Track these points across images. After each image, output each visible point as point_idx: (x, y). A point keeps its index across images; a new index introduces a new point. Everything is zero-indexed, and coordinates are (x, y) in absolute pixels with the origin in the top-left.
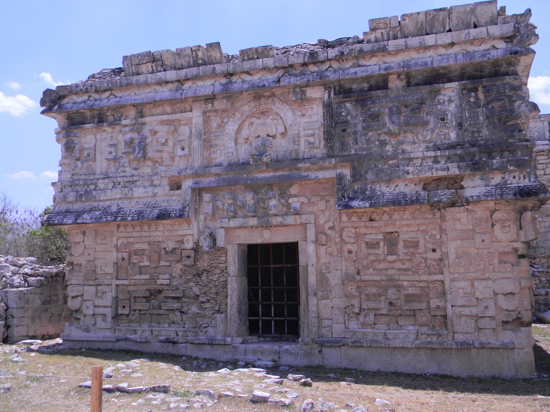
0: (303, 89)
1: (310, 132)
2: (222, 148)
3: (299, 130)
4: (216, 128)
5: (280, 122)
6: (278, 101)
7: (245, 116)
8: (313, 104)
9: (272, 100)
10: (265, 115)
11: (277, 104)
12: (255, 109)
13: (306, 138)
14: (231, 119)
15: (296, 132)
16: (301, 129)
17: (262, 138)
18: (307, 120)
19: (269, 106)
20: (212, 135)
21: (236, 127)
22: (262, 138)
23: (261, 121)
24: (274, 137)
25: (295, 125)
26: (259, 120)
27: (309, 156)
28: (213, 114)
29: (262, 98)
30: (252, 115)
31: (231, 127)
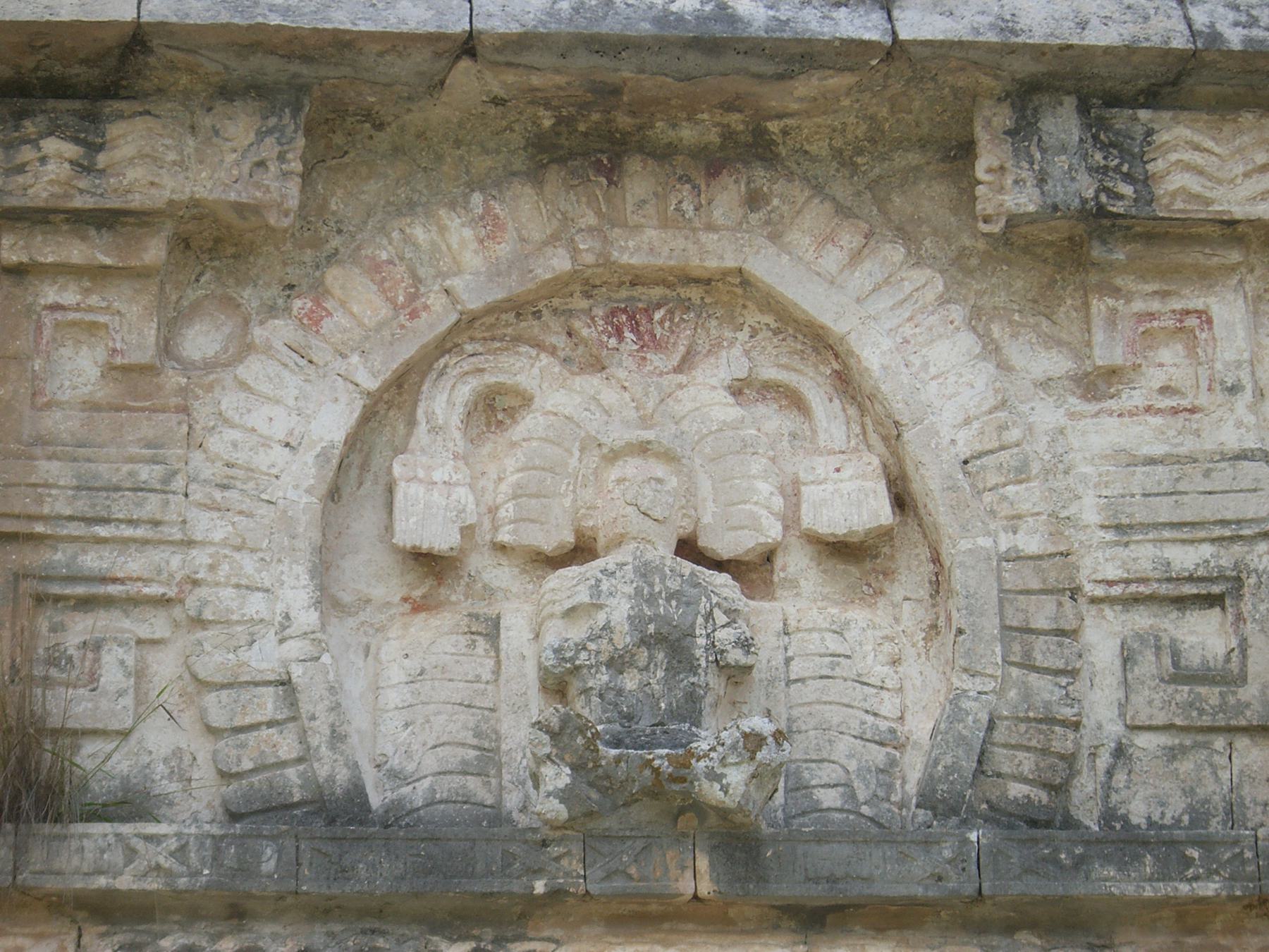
0: (1120, 118)
1: (1186, 558)
2: (155, 625)
3: (1059, 523)
4: (92, 406)
5: (830, 418)
6: (816, 214)
7: (438, 316)
8: (1206, 277)
9: (754, 200)
10: (649, 342)
11: (801, 238)
12: (560, 262)
13: (1142, 619)
14: (279, 331)
15: (1031, 544)
16: (1089, 511)
17: (645, 571)
18: (1148, 436)
19: (716, 252)
20: (50, 469)
21: (333, 422)
22: (645, 571)
23: (610, 396)
24: (754, 571)
25: (1021, 474)
26: (593, 382)
27: (1177, 806)
28: (76, 252)
29: (634, 164)
30: (511, 318)
31: (279, 409)
